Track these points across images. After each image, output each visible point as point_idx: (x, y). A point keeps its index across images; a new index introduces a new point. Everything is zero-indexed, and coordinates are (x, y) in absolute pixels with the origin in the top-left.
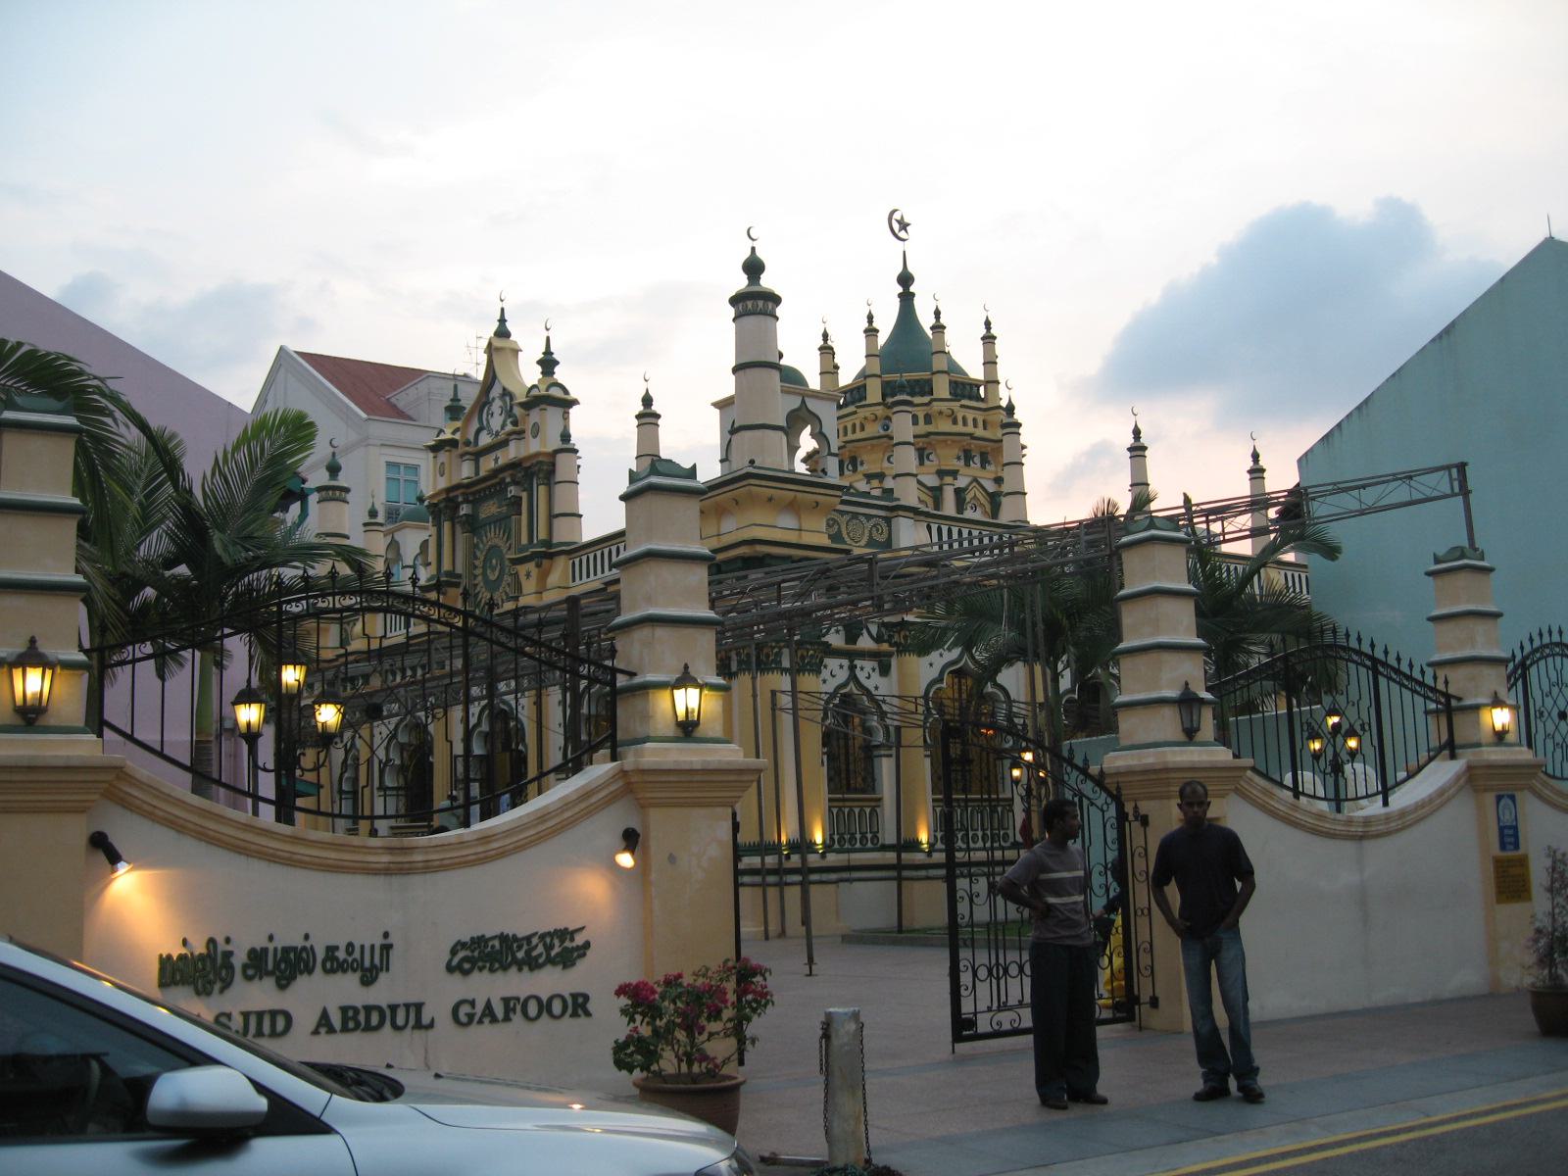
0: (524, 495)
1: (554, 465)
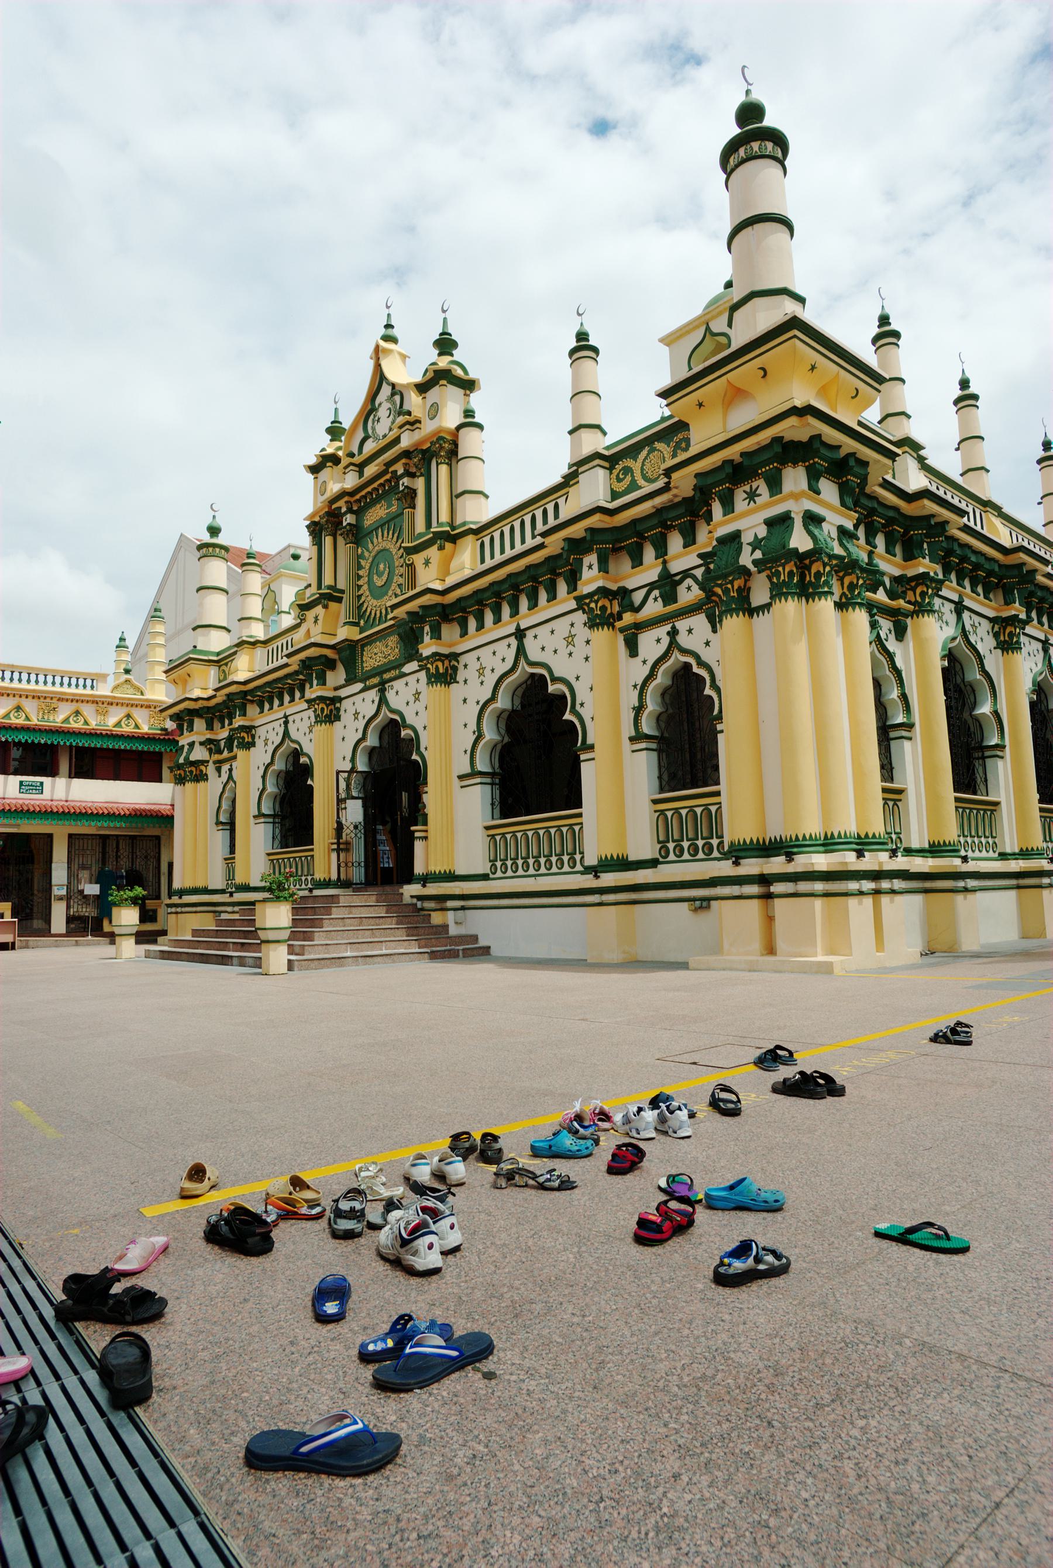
0: (420, 484)
1: (456, 446)
